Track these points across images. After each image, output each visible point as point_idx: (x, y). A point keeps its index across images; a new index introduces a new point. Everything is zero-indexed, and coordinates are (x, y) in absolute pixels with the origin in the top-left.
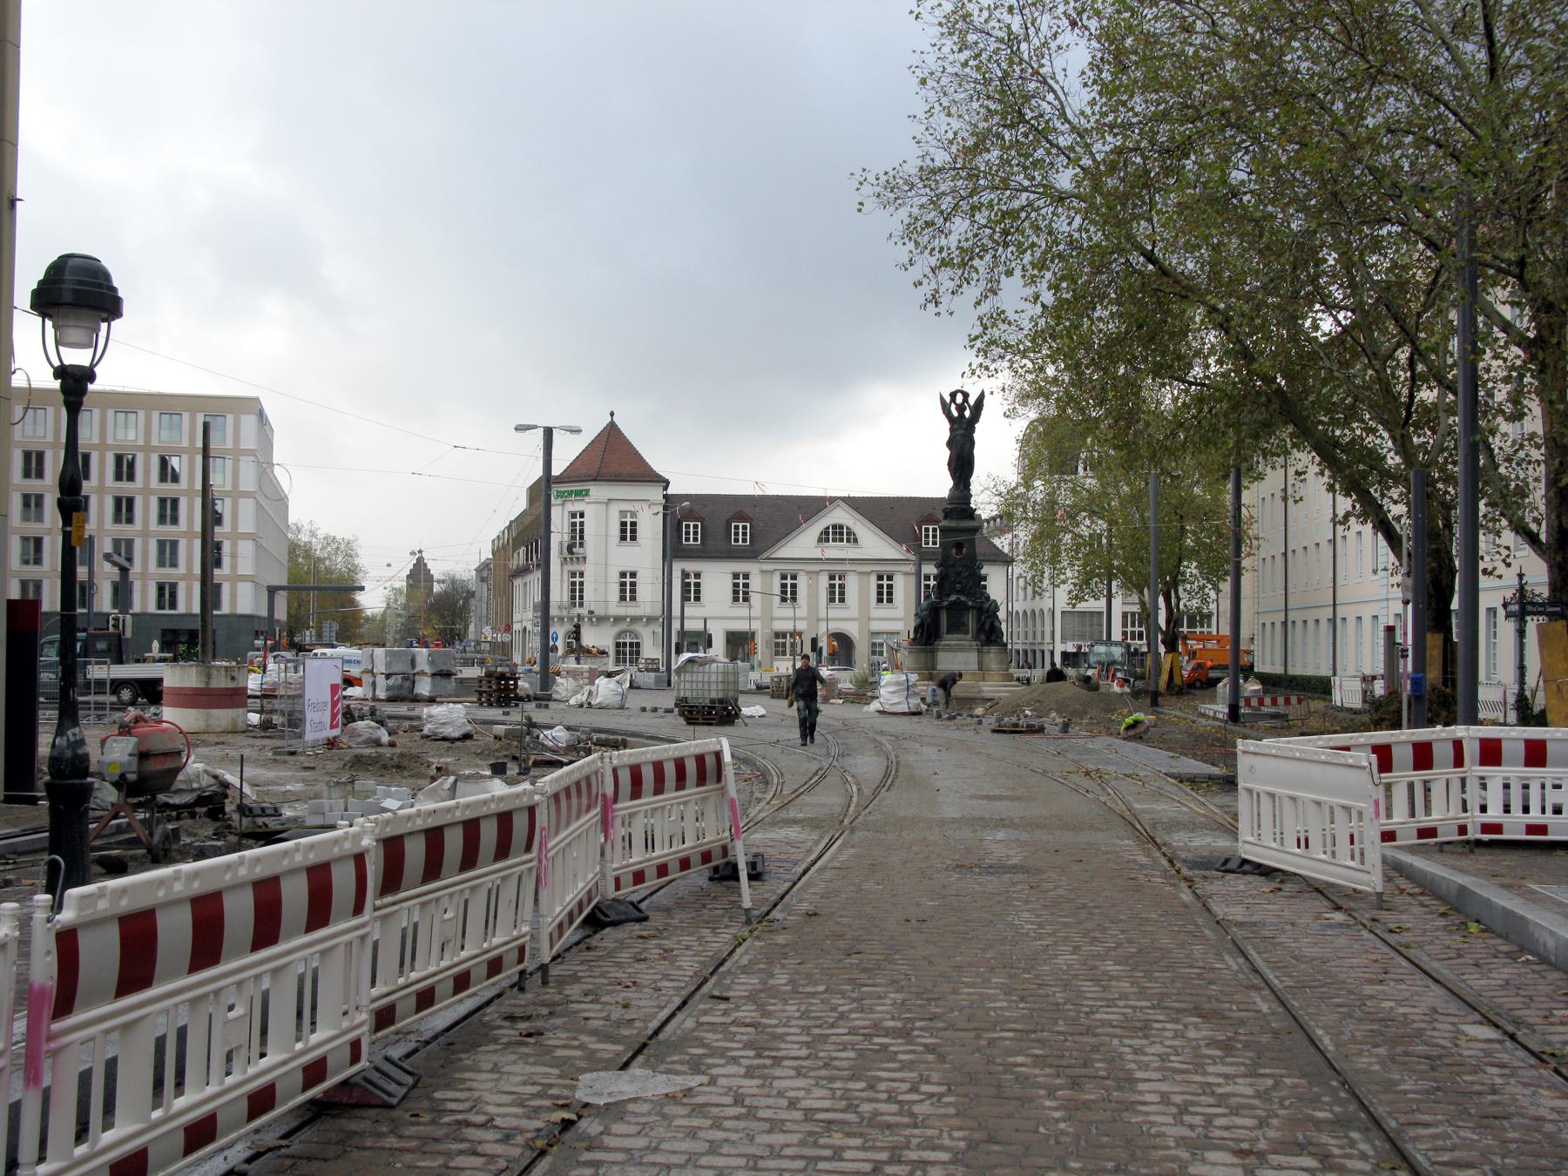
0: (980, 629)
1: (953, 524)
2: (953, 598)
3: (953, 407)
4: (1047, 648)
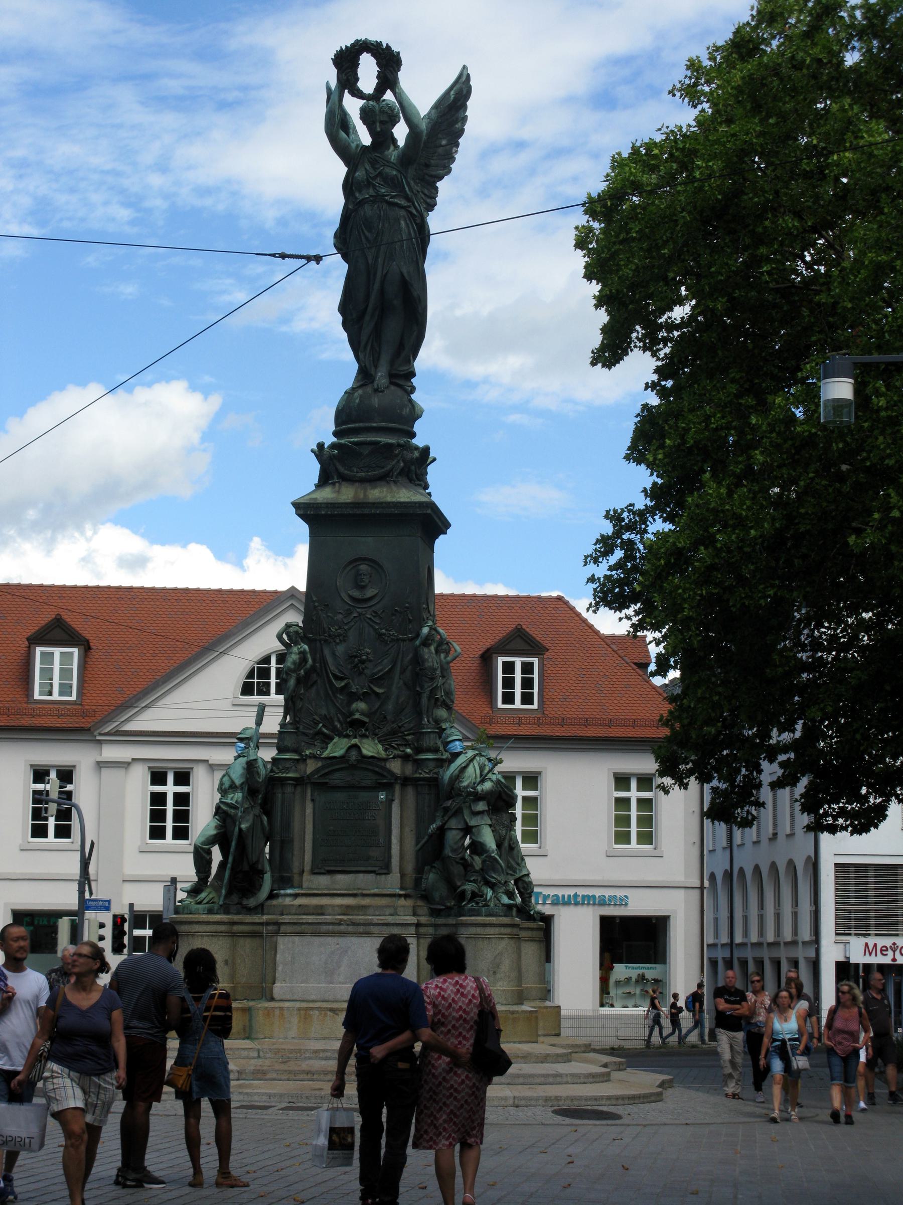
0: (432, 851)
1: (347, 494)
2: (337, 748)
3: (353, 106)
4: (802, 954)
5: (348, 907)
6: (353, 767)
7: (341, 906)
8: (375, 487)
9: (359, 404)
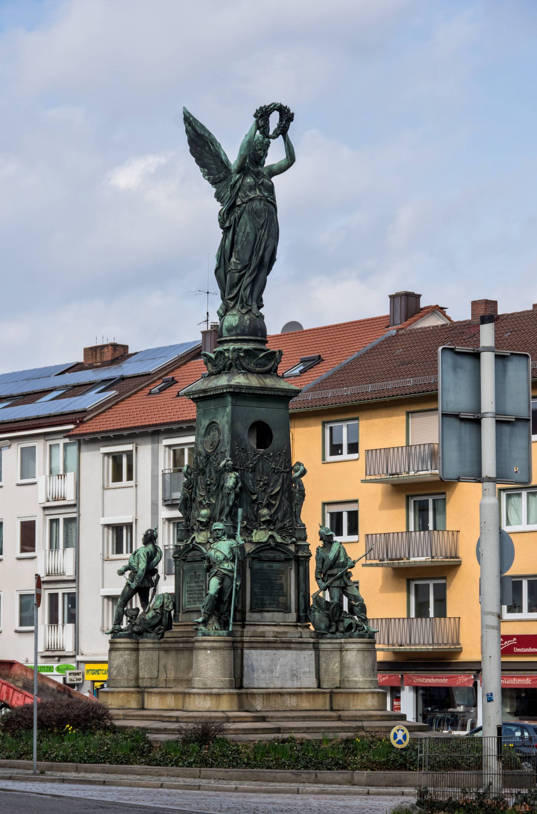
5: (277, 632)
6: (273, 549)
7: (273, 632)
8: (266, 378)
9: (250, 325)
